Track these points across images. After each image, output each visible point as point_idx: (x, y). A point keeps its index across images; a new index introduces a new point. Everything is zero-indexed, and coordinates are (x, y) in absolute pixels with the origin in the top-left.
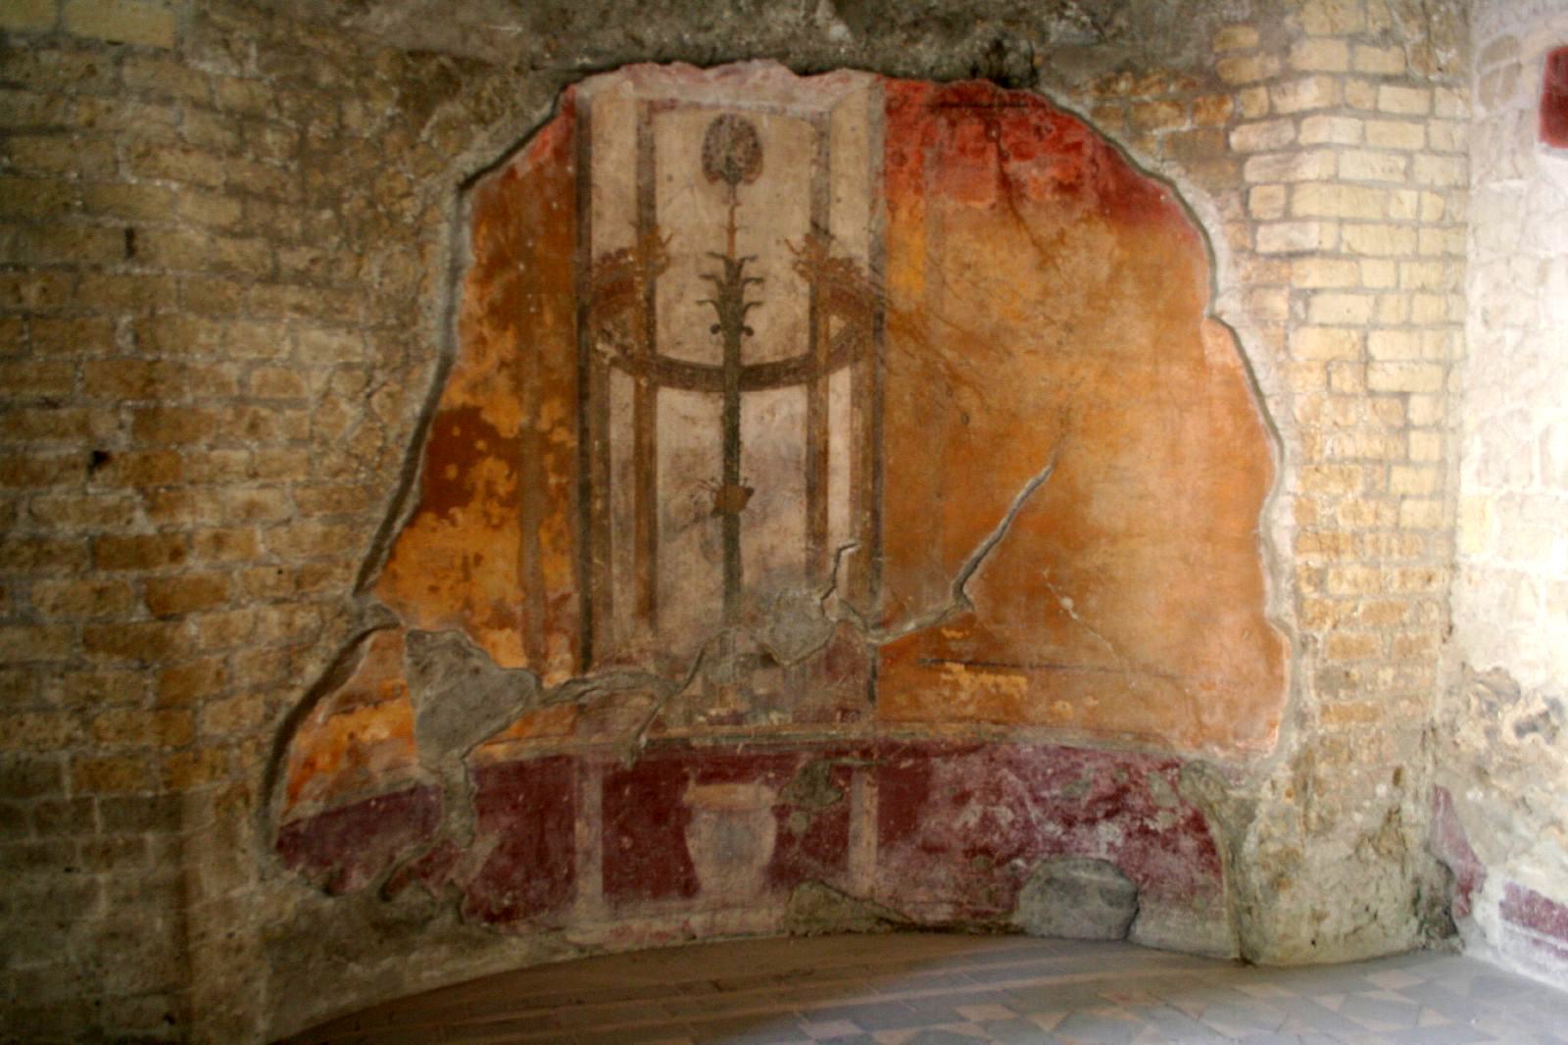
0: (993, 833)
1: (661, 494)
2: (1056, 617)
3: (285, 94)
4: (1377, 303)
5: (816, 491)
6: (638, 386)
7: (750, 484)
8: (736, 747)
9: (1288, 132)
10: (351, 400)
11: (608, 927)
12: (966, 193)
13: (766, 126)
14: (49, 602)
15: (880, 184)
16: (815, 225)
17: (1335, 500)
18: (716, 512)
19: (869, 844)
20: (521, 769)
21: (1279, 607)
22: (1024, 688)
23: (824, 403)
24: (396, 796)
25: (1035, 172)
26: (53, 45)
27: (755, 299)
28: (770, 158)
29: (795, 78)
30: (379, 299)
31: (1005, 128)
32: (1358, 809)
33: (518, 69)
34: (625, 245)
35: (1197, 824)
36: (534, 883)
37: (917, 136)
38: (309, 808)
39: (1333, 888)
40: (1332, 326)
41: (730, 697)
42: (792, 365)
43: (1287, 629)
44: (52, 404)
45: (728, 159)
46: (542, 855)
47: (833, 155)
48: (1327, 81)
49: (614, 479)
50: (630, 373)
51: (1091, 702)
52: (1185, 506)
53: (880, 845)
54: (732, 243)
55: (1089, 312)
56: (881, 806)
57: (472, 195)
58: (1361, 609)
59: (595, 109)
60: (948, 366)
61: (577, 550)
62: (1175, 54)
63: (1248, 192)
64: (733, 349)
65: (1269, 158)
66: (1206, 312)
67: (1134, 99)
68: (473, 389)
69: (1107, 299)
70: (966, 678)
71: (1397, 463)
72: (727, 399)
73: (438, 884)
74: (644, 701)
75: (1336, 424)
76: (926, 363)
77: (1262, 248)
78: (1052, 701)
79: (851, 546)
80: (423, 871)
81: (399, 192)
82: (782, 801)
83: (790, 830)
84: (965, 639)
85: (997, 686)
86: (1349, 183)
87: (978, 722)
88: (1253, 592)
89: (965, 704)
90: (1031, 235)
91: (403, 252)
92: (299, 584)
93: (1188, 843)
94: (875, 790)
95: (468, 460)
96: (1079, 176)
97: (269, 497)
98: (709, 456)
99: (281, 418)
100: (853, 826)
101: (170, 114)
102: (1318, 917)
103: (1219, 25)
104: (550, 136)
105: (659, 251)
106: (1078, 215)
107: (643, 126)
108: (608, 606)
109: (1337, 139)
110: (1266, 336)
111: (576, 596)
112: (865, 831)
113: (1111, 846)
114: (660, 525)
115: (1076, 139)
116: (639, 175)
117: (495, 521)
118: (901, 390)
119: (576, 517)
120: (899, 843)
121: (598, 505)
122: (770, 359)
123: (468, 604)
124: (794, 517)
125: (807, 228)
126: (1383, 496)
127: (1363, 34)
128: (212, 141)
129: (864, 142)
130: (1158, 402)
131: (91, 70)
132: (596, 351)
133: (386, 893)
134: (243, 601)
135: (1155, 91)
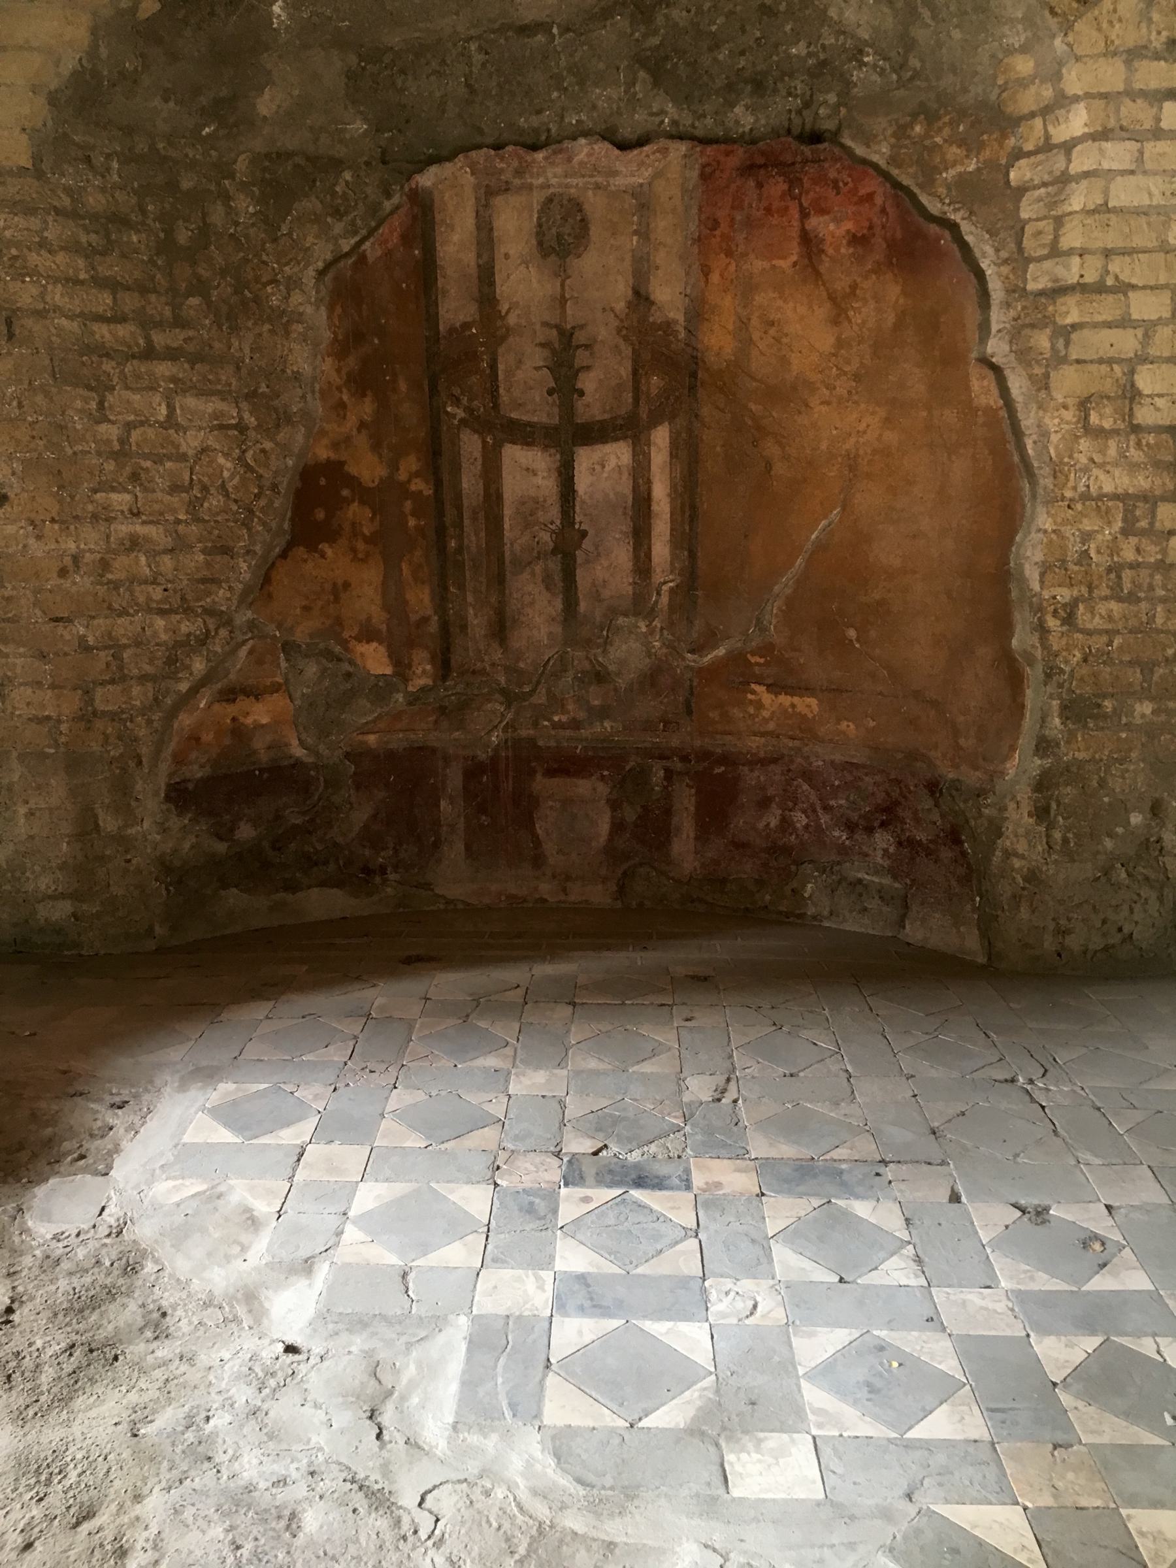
0: (791, 834)
3: (148, 199)
4: (1146, 335)
5: (640, 534)
6: (484, 442)
8: (576, 748)
10: (226, 455)
13: (595, 204)
15: (695, 250)
16: (637, 293)
17: (1086, 537)
18: (554, 551)
19: (688, 836)
20: (391, 755)
21: (1022, 639)
22: (816, 709)
25: (832, 227)
27: (585, 364)
28: (595, 232)
29: (617, 152)
33: (367, 164)
34: (469, 319)
35: (954, 837)
36: (405, 846)
38: (196, 771)
40: (1092, 362)
42: (620, 422)
43: (1031, 661)
47: (652, 225)
48: (1099, 104)
49: (466, 522)
51: (872, 724)
53: (697, 838)
57: (328, 278)
58: (1115, 644)
59: (436, 196)
62: (965, 90)
63: (1023, 229)
64: (568, 409)
65: (1043, 190)
66: (974, 355)
67: (927, 143)
68: (335, 446)
70: (767, 698)
71: (1164, 499)
75: (1092, 460)
77: (1031, 286)
78: (838, 721)
79: (671, 581)
81: (264, 280)
84: (767, 664)
85: (793, 706)
87: (778, 737)
88: (1003, 626)
90: (827, 290)
91: (270, 330)
92: (183, 598)
93: (946, 854)
94: (693, 791)
96: (871, 228)
97: (152, 531)
98: (549, 502)
99: (161, 469)
100: (675, 820)
101: (35, 223)
102: (1062, 932)
103: (1001, 56)
104: (397, 223)
105: (499, 323)
107: (481, 209)
108: (464, 628)
111: (436, 618)
113: (885, 851)
115: (869, 190)
116: (479, 256)
117: (360, 556)
123: (339, 621)
124: (622, 555)
126: (1148, 532)
128: (78, 242)
132: (447, 413)
134: (131, 611)
135: (946, 131)
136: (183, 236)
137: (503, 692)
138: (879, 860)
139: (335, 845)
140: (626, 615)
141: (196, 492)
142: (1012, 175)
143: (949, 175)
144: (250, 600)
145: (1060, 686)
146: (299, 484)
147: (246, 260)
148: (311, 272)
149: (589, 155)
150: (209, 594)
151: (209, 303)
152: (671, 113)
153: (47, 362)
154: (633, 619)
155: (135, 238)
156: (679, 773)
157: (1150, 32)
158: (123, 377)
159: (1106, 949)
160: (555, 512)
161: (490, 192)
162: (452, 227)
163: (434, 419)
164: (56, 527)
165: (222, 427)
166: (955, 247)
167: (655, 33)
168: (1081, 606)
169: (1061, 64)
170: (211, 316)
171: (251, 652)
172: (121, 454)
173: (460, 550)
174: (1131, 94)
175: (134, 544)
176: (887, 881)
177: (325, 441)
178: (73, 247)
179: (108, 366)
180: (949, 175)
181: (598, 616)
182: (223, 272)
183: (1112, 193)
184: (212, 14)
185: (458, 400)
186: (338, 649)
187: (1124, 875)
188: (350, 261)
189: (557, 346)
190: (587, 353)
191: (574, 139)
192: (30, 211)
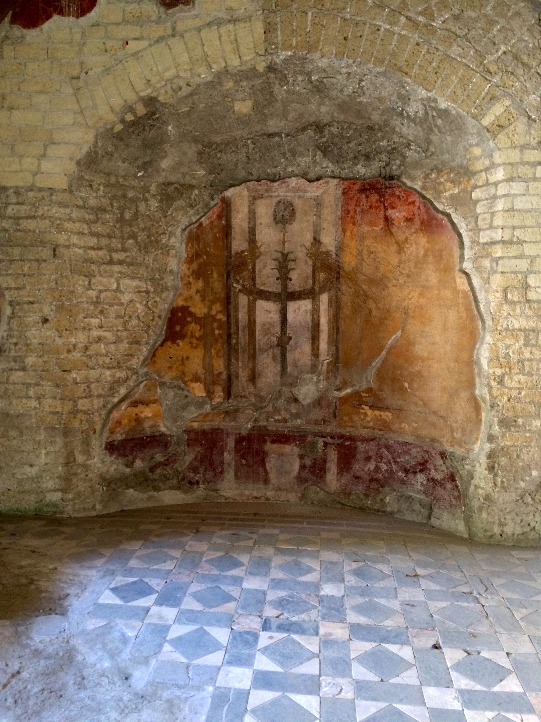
1: (257, 337)
2: (403, 390)
3: (114, 201)
5: (315, 339)
6: (249, 299)
9: (492, 191)
10: (141, 303)
11: (236, 492)
12: (372, 224)
13: (298, 203)
14: (30, 364)
15: (340, 222)
16: (315, 239)
17: (508, 347)
18: (278, 345)
20: (204, 432)
21: (481, 391)
22: (390, 417)
23: (318, 306)
24: (154, 436)
25: (397, 214)
26: (32, 190)
28: (298, 215)
29: (308, 183)
30: (152, 270)
31: (387, 197)
32: (523, 480)
33: (205, 187)
35: (452, 478)
37: (354, 203)
38: (119, 437)
39: (509, 512)
41: (283, 413)
44: (32, 303)
45: (283, 216)
46: (211, 464)
49: (240, 332)
50: (246, 294)
51: (415, 425)
52: (448, 347)
53: (338, 474)
54: (284, 246)
55: (416, 270)
56: (338, 458)
57: (186, 233)
58: (523, 394)
59: (232, 200)
60: (363, 291)
61: (226, 356)
62: (453, 161)
63: (478, 217)
64: (285, 286)
65: (486, 202)
67: (438, 181)
68: (186, 300)
69: (423, 264)
70: (369, 412)
72: (282, 304)
73: (170, 468)
74: (251, 412)
75: (509, 314)
76: (356, 291)
77: (482, 241)
78: (400, 423)
80: (165, 464)
82: (301, 453)
83: (304, 464)
84: (369, 396)
85: (381, 416)
86: (519, 211)
88: (471, 385)
89: (369, 422)
92: (118, 363)
93: (449, 486)
94: (336, 452)
95: (184, 324)
96: (414, 215)
97: (107, 334)
99: (112, 308)
100: (328, 465)
101: (68, 211)
102: (503, 525)
104: (216, 210)
105: (257, 250)
106: (413, 230)
108: (237, 377)
109: (512, 192)
110: (481, 278)
111: (225, 373)
112: (332, 468)
113: (422, 483)
114: (257, 349)
115: (413, 200)
116: (249, 223)
118: (346, 300)
119: (225, 346)
120: (345, 474)
121: (234, 341)
122: (298, 290)
123: (183, 373)
124: (307, 348)
125: (312, 240)
127: (528, 144)
129: (334, 207)
130: (440, 305)
131: (43, 198)
133: (152, 470)
135: (445, 177)
136: (128, 216)
137: (253, 405)
138: (419, 487)
139: (177, 471)
140: (308, 373)
141: (126, 318)
142: (473, 195)
143: (447, 194)
144: (146, 363)
145: (498, 411)
146: (169, 315)
147: (153, 225)
148: (179, 230)
149: (296, 184)
150: (129, 360)
151: (137, 242)
152: (330, 167)
153: (68, 266)
154: (310, 375)
155: (108, 216)
156: (330, 444)
157: (530, 138)
158: (99, 271)
159: (523, 534)
161: (255, 199)
162: (238, 212)
163: (228, 288)
164: (67, 332)
165: (140, 292)
166: (449, 224)
167: (324, 137)
168: (506, 377)
169: (492, 151)
170: (138, 248)
171: (145, 386)
172: (96, 303)
173: (237, 343)
174: (523, 163)
175: (99, 339)
176: (423, 497)
177: (182, 298)
178: (83, 221)
179: (93, 267)
180: (447, 194)
181: (296, 373)
182: (143, 230)
183: (515, 204)
184: (144, 130)
185: (238, 281)
186: (182, 385)
187: (530, 499)
188: (196, 225)
189: (281, 259)
190: (293, 263)
191: (290, 177)
192: (67, 206)
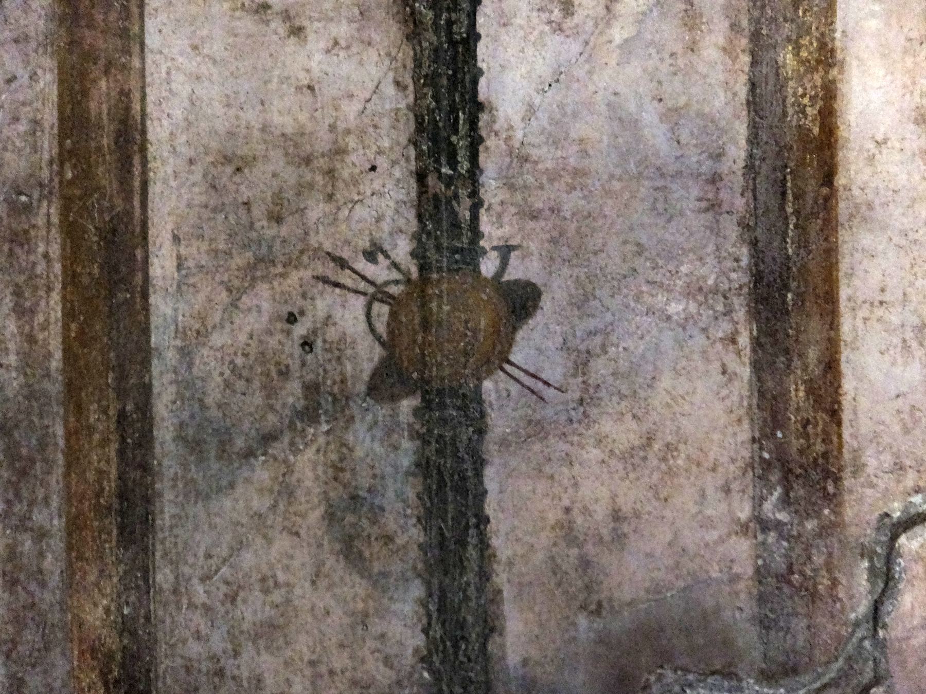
7: (516, 272)
98: (357, 159)
160: (387, 205)
